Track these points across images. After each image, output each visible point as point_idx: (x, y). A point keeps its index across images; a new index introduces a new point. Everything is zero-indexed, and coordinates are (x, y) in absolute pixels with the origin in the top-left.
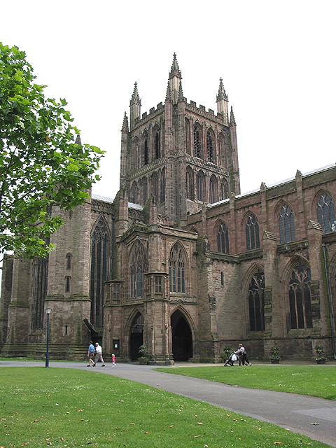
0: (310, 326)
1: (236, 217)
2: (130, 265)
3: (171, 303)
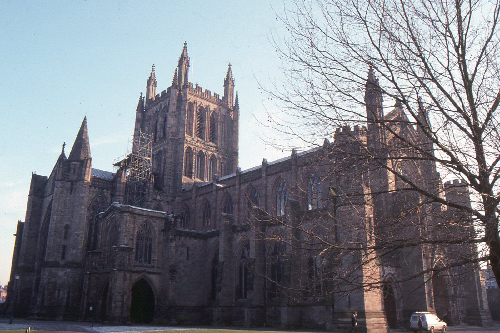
0: (246, 297)
2: (108, 238)
3: (137, 272)
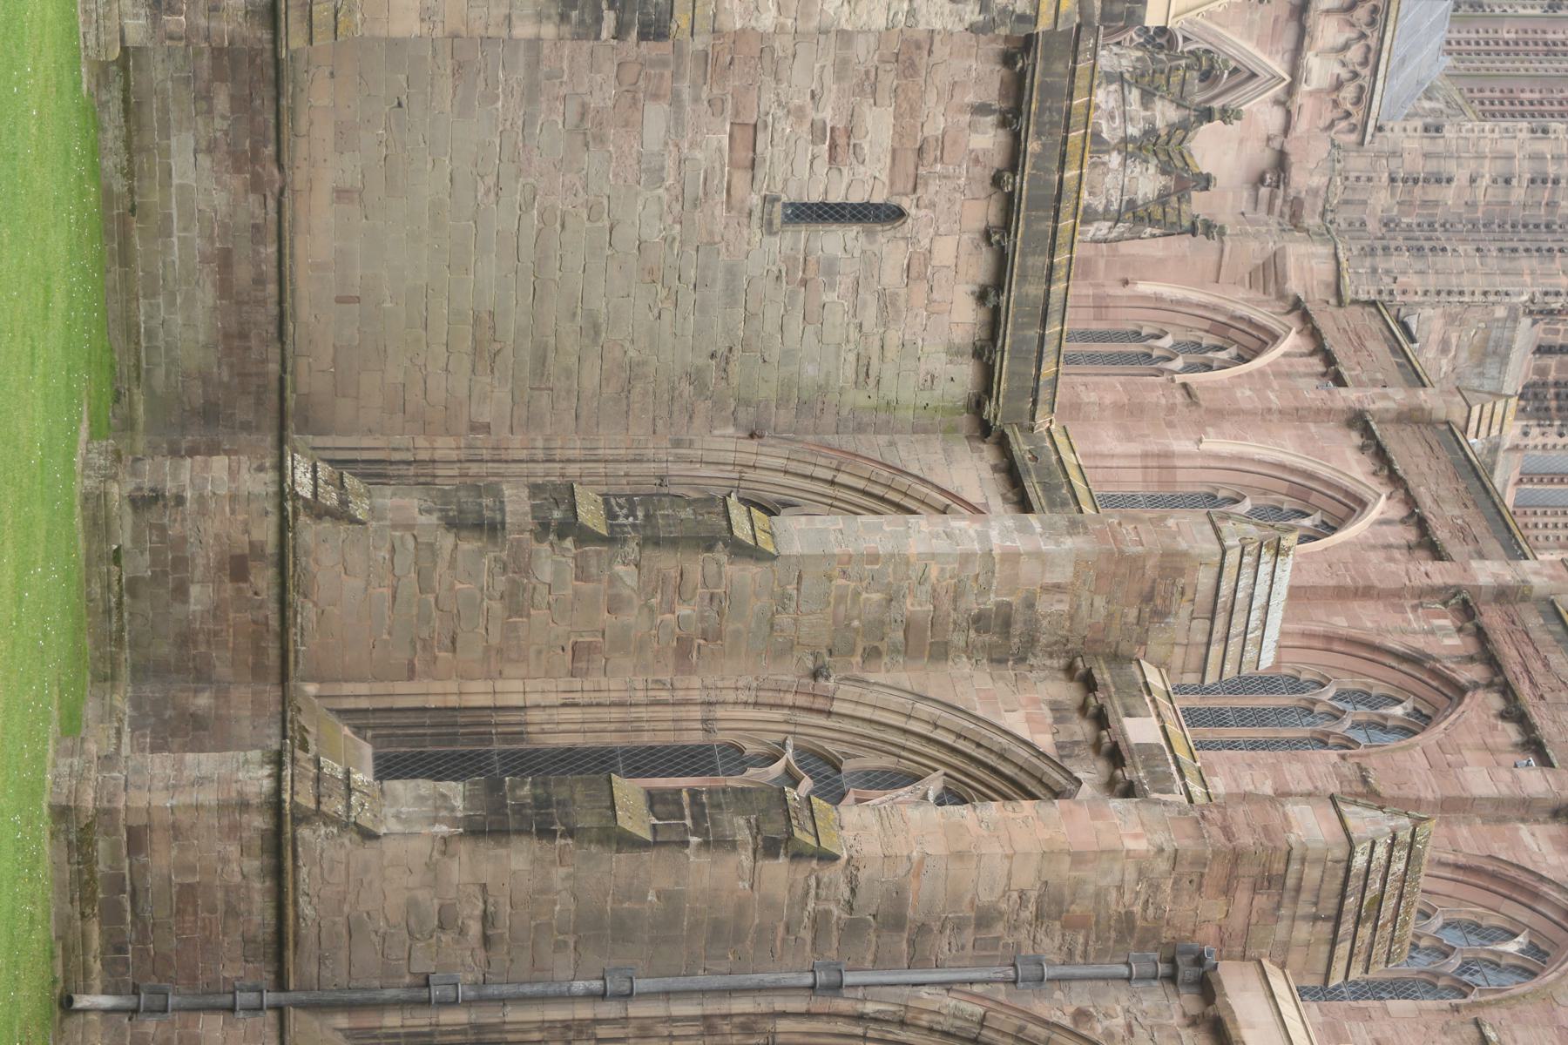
1: (1393, 596)
